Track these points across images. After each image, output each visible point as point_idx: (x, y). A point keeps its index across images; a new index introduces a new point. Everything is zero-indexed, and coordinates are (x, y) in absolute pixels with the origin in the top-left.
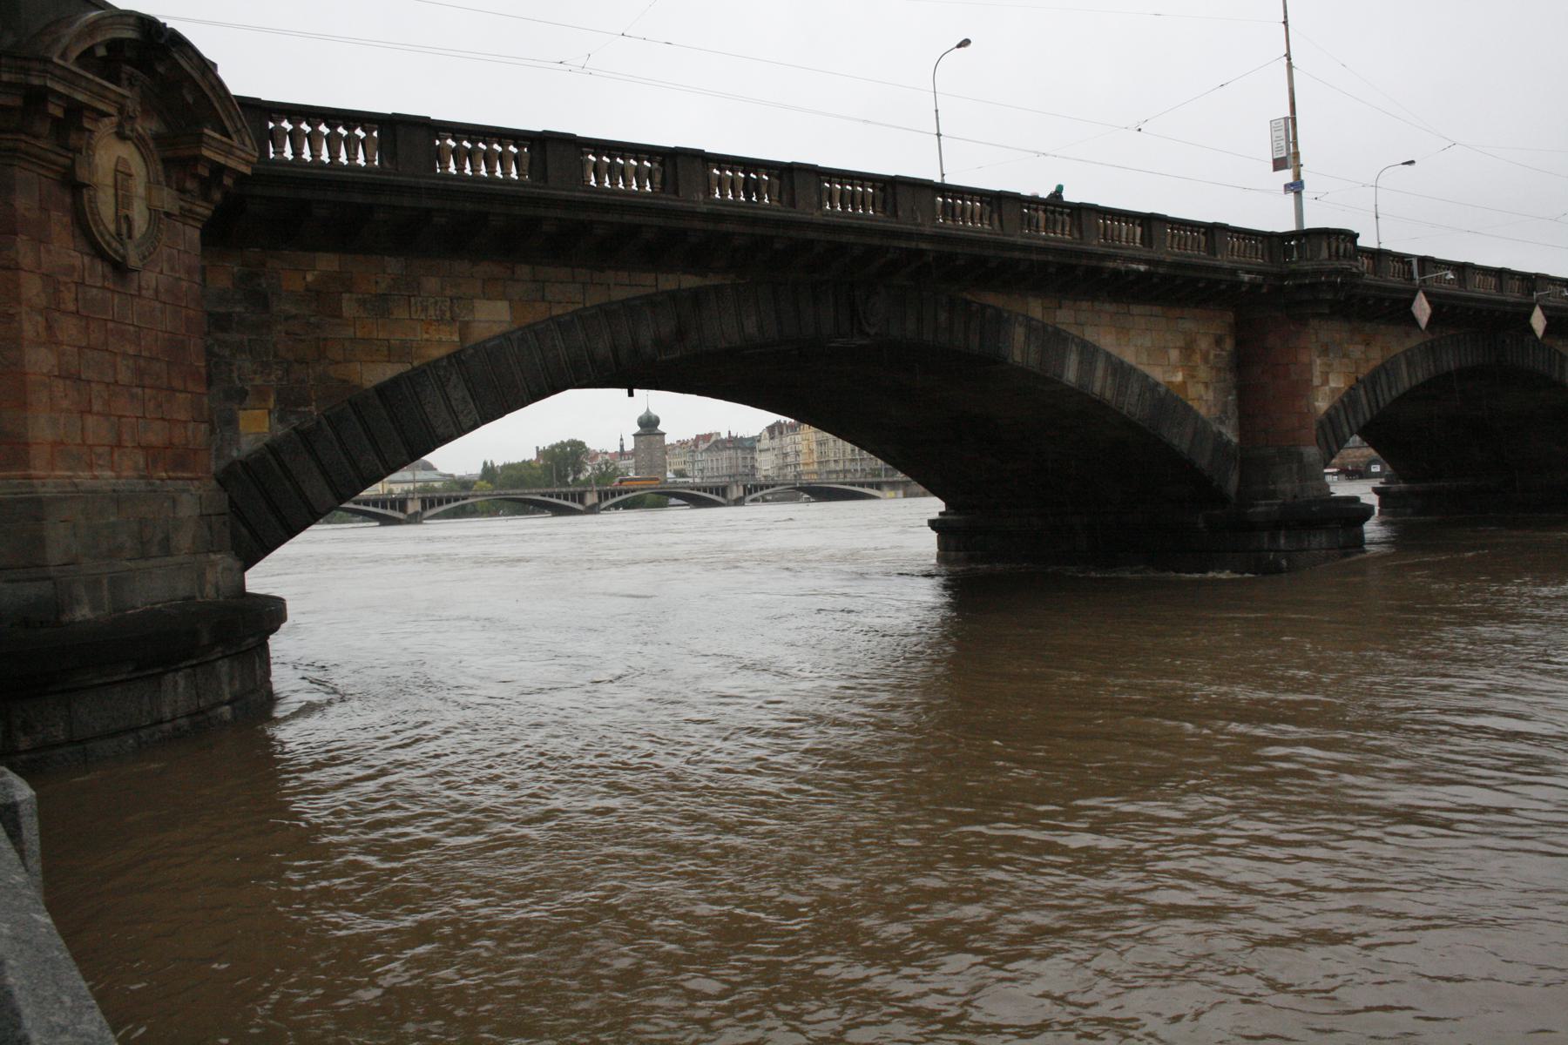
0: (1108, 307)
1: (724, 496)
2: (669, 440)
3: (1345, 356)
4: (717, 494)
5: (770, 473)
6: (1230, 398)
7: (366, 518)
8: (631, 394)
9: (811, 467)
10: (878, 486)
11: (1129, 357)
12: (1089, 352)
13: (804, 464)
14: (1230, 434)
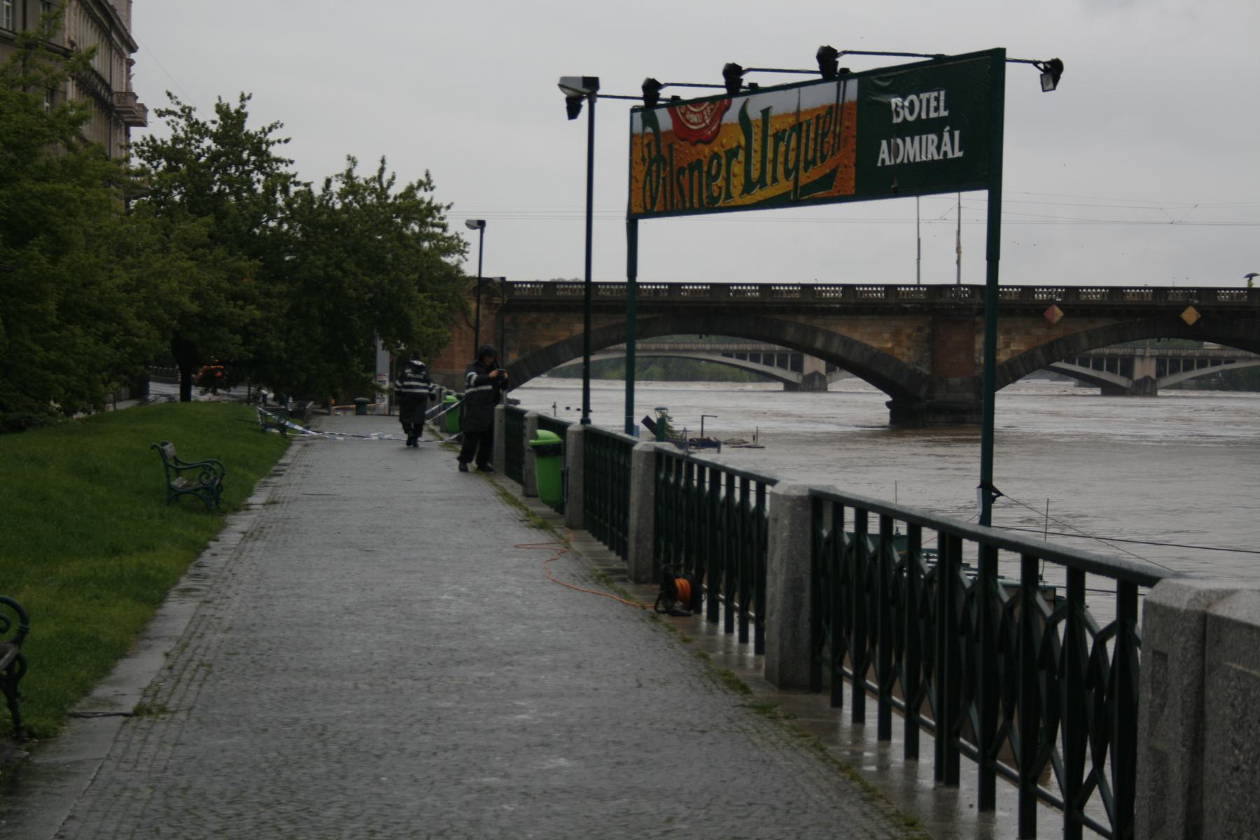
3: (1028, 333)
6: (926, 354)
7: (1063, 376)
11: (856, 336)
12: (830, 336)
14: (925, 370)
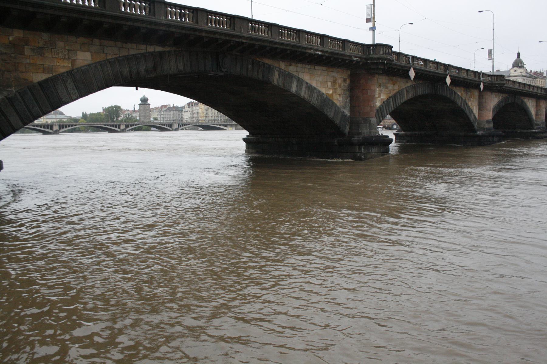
0: (307, 66)
1: (171, 127)
2: (152, 106)
3: (387, 88)
4: (169, 127)
5: (188, 120)
8: (137, 89)
9: (203, 118)
10: (226, 126)
11: (314, 84)
12: (300, 81)
13: (200, 117)
